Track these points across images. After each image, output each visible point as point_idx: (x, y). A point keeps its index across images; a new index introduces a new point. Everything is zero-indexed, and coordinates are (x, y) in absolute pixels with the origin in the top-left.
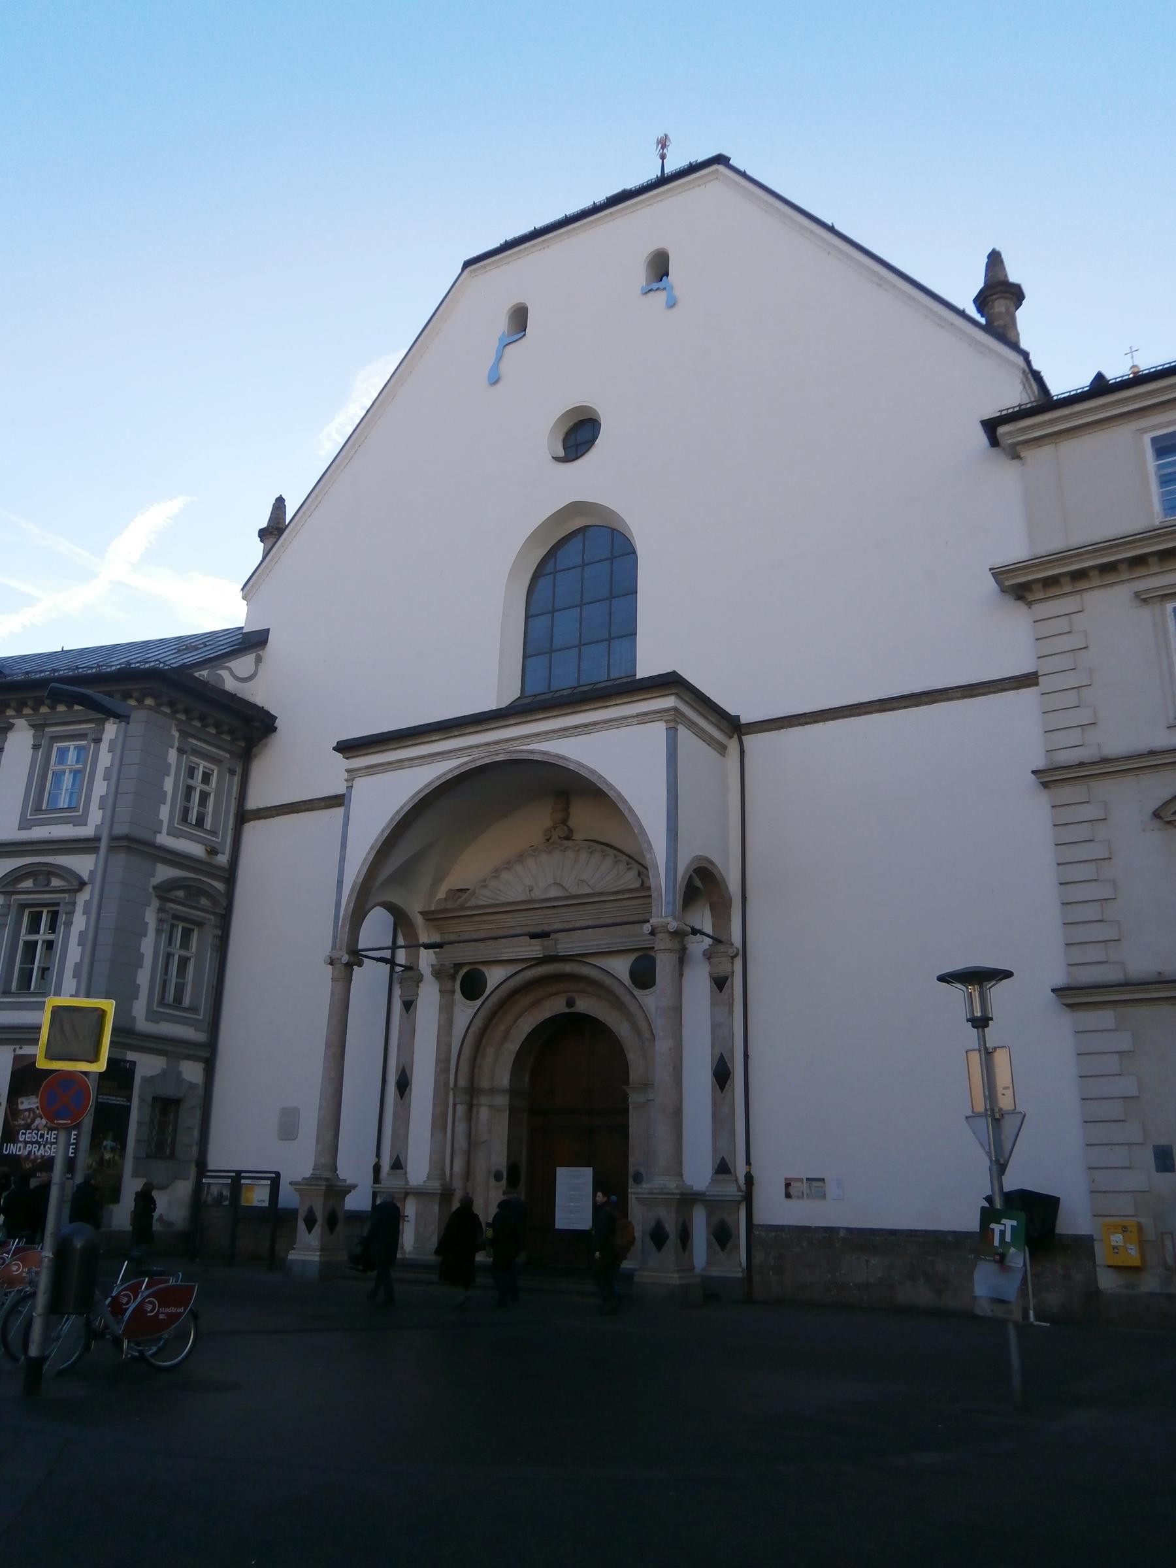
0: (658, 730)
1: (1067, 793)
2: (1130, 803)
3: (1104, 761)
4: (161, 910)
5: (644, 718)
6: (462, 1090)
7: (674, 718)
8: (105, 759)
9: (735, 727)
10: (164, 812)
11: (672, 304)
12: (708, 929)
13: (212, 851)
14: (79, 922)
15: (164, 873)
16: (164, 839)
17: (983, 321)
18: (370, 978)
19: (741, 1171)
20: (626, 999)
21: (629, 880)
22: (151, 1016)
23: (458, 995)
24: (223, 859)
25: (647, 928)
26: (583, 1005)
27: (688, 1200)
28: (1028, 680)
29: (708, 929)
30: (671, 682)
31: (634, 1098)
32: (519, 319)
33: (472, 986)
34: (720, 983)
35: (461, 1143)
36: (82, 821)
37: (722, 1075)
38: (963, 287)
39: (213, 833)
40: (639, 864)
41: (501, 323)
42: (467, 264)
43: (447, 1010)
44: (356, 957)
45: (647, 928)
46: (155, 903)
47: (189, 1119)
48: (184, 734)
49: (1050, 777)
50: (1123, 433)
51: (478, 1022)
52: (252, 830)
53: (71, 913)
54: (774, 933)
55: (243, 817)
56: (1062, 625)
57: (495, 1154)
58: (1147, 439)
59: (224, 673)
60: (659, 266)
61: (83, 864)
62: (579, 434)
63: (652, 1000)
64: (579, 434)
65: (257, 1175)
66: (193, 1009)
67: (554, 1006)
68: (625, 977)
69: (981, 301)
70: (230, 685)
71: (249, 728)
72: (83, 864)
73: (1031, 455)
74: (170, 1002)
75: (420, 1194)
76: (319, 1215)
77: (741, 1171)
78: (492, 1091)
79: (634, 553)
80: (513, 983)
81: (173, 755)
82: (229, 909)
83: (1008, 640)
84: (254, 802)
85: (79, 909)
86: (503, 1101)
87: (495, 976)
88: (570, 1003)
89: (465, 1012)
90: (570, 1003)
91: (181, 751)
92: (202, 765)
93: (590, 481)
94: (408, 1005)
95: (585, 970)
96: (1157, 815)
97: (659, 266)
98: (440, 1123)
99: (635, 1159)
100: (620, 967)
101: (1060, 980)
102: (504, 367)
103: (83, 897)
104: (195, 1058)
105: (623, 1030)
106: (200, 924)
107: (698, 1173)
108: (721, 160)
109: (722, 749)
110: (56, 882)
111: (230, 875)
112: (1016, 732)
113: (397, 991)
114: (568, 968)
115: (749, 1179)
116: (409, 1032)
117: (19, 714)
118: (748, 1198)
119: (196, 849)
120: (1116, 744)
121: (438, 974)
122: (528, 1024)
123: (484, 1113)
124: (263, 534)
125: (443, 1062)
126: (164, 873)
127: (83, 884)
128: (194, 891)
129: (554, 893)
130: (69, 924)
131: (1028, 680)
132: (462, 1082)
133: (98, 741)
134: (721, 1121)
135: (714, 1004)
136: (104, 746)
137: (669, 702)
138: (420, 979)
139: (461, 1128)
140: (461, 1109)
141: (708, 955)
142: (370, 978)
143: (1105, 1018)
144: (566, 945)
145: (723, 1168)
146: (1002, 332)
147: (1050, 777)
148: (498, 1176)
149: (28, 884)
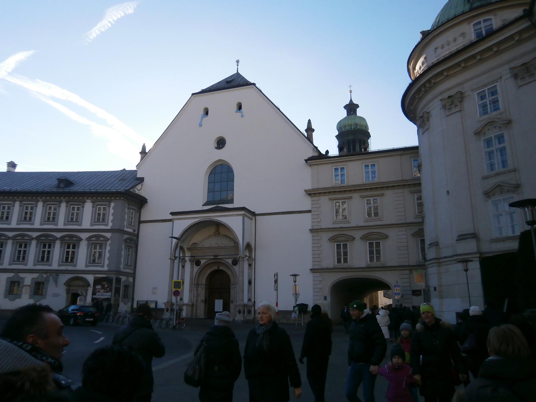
0: (241, 218)
1: (315, 234)
3: (321, 229)
4: (125, 245)
5: (238, 215)
6: (195, 284)
7: (244, 216)
8: (112, 211)
9: (254, 214)
10: (125, 223)
11: (242, 116)
12: (248, 255)
13: (134, 231)
14: (108, 248)
15: (126, 236)
16: (126, 229)
17: (306, 134)
18: (176, 261)
19: (253, 300)
20: (231, 267)
21: (232, 244)
22: (124, 268)
23: (195, 265)
24: (136, 232)
25: (238, 256)
26: (221, 268)
27: (245, 305)
28: (309, 211)
29: (248, 255)
30: (243, 209)
31: (232, 286)
32: (206, 112)
33: (198, 263)
34: (250, 265)
35: (195, 295)
36: (107, 225)
37: (250, 283)
38: (303, 128)
39: (134, 226)
40: (236, 243)
41: (202, 112)
42: (193, 94)
43: (192, 268)
44: (176, 257)
45: (238, 256)
46: (124, 243)
47: (130, 290)
48: (129, 205)
49: (312, 231)
50: (329, 166)
51: (199, 271)
52: (142, 225)
53: (106, 246)
54: (260, 256)
55: (140, 222)
56: (316, 202)
57: (202, 297)
59: (136, 189)
60: (240, 107)
61: (108, 235)
62: (221, 143)
63: (236, 268)
64: (221, 143)
65: (152, 302)
66: (131, 266)
67: (215, 268)
68: (231, 263)
69: (306, 130)
70: (137, 192)
71: (141, 202)
72: (108, 235)
73: (313, 167)
74: (127, 265)
75: (186, 305)
76: (169, 309)
77: (253, 300)
78: (202, 284)
79: (233, 172)
80: (207, 263)
81: (127, 209)
82: (138, 243)
83: (306, 203)
84: (142, 219)
85: (108, 245)
86: (204, 286)
87: (203, 262)
88: (218, 267)
89: (196, 269)
90: (218, 267)
91: (128, 209)
92: (132, 211)
93: (223, 155)
94: (183, 267)
95: (223, 261)
96: (329, 239)
97: (240, 107)
98: (191, 291)
99: (232, 298)
100: (230, 261)
101: (311, 268)
102: (203, 122)
103: (109, 242)
104: (131, 276)
105: (229, 273)
106: (132, 247)
107: (246, 301)
108: (254, 84)
109: (251, 219)
110: (101, 239)
111: (137, 236)
112: (306, 221)
113: (180, 264)
114: (219, 261)
115: (254, 302)
116: (183, 272)
117: (88, 199)
118: (254, 305)
119: (131, 230)
120: (323, 226)
121: (190, 261)
122: (209, 271)
123: (200, 289)
124: (141, 153)
125: (191, 279)
126: (126, 236)
127: (109, 239)
128: (131, 240)
129: (216, 246)
130: (106, 248)
131: (309, 211)
132: (196, 283)
133: (110, 207)
134: (249, 291)
135: (249, 269)
136: (111, 208)
137: (243, 212)
138: (186, 261)
139: (195, 292)
140: (195, 288)
141: (248, 260)
142: (176, 261)
143: (318, 274)
144: (219, 257)
145: (249, 300)
146: (310, 139)
147: (312, 231)
148: (203, 301)
149: (94, 239)
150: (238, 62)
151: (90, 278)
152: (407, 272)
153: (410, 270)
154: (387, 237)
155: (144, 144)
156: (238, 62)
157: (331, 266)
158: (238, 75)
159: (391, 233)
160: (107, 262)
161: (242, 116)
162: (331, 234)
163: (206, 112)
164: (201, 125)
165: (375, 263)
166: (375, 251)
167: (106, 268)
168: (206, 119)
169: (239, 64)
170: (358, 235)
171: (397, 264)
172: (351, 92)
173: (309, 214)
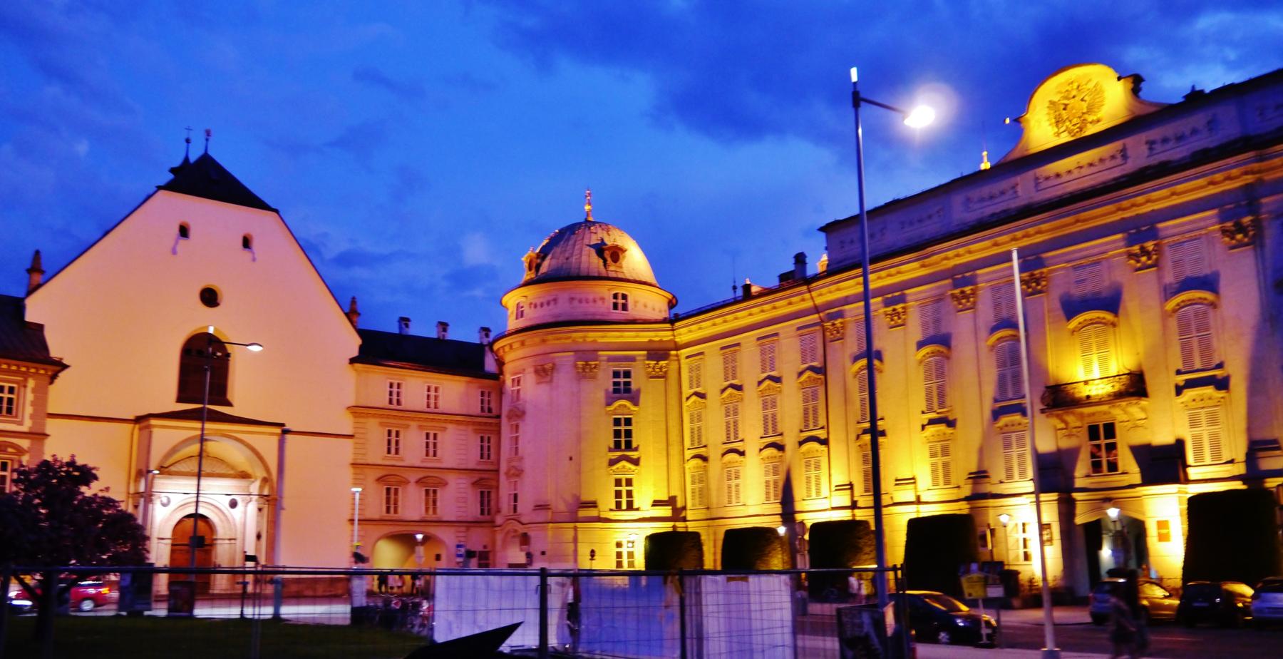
2: (373, 474)
8: (30, 397)
11: (254, 260)
28: (351, 436)
32: (184, 231)
36: (21, 423)
41: (176, 230)
49: (354, 465)
60: (247, 243)
83: (346, 424)
97: (247, 243)
102: (179, 249)
108: (276, 211)
110: (10, 450)
120: (370, 462)
131: (351, 436)
133: (25, 387)
136: (29, 390)
147: (354, 465)
150: (208, 133)
152: (463, 529)
153: (468, 528)
154: (445, 484)
155: (37, 253)
156: (208, 133)
157: (377, 517)
158: (206, 159)
159: (451, 478)
161: (254, 260)
163: (184, 231)
164: (174, 252)
165: (431, 516)
166: (431, 499)
168: (183, 242)
169: (211, 139)
170: (413, 477)
171: (453, 519)
172: (188, 141)
173: (350, 441)
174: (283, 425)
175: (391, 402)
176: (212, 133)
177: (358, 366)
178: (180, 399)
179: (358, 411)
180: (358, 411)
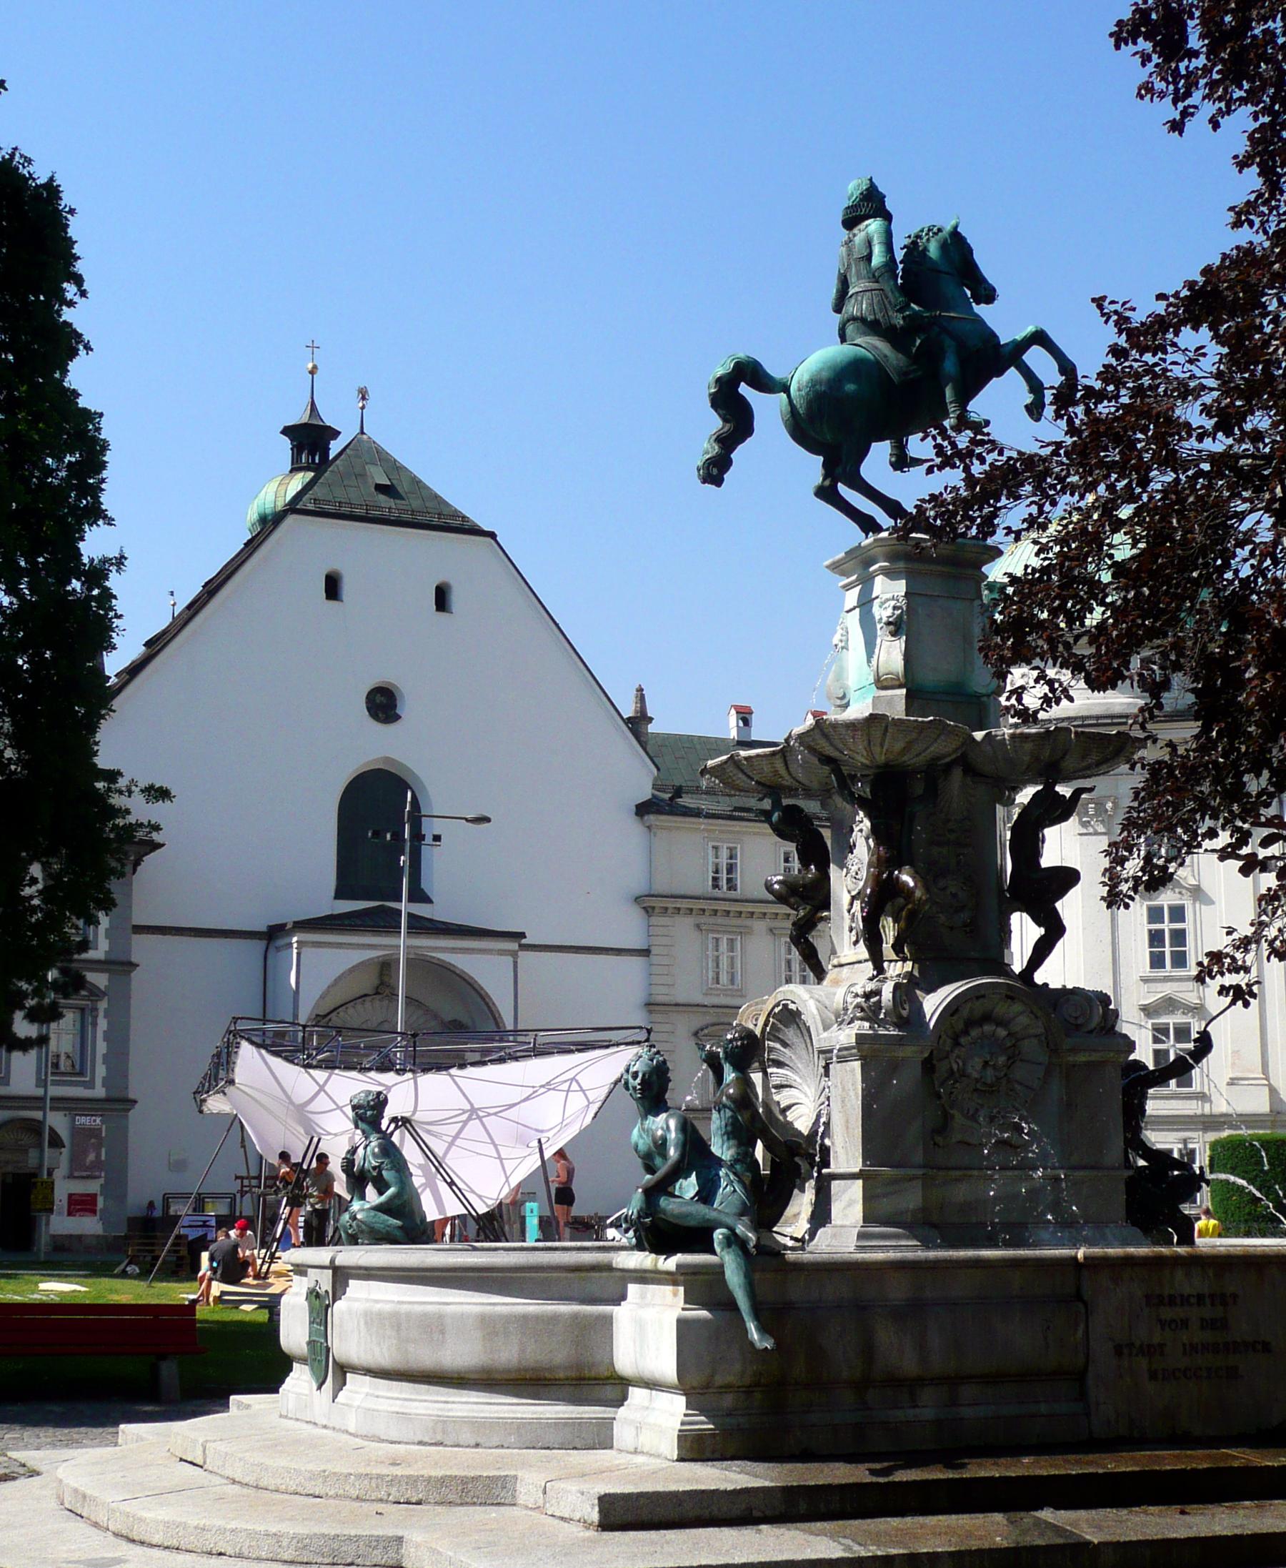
5: (502, 952)
14: (102, 1024)
58: (711, 844)
85: (101, 1014)
103: (103, 1005)
108: (492, 535)
120: (681, 1000)
130: (95, 1024)
147: (648, 1004)
150: (363, 395)
151: (57, 1121)
156: (363, 395)
160: (101, 1071)
162: (697, 1021)
167: (99, 1092)
169: (369, 404)
173: (637, 961)
174: (522, 935)
175: (716, 884)
176: (371, 394)
177: (651, 818)
178: (340, 894)
179: (652, 904)
180: (652, 904)
